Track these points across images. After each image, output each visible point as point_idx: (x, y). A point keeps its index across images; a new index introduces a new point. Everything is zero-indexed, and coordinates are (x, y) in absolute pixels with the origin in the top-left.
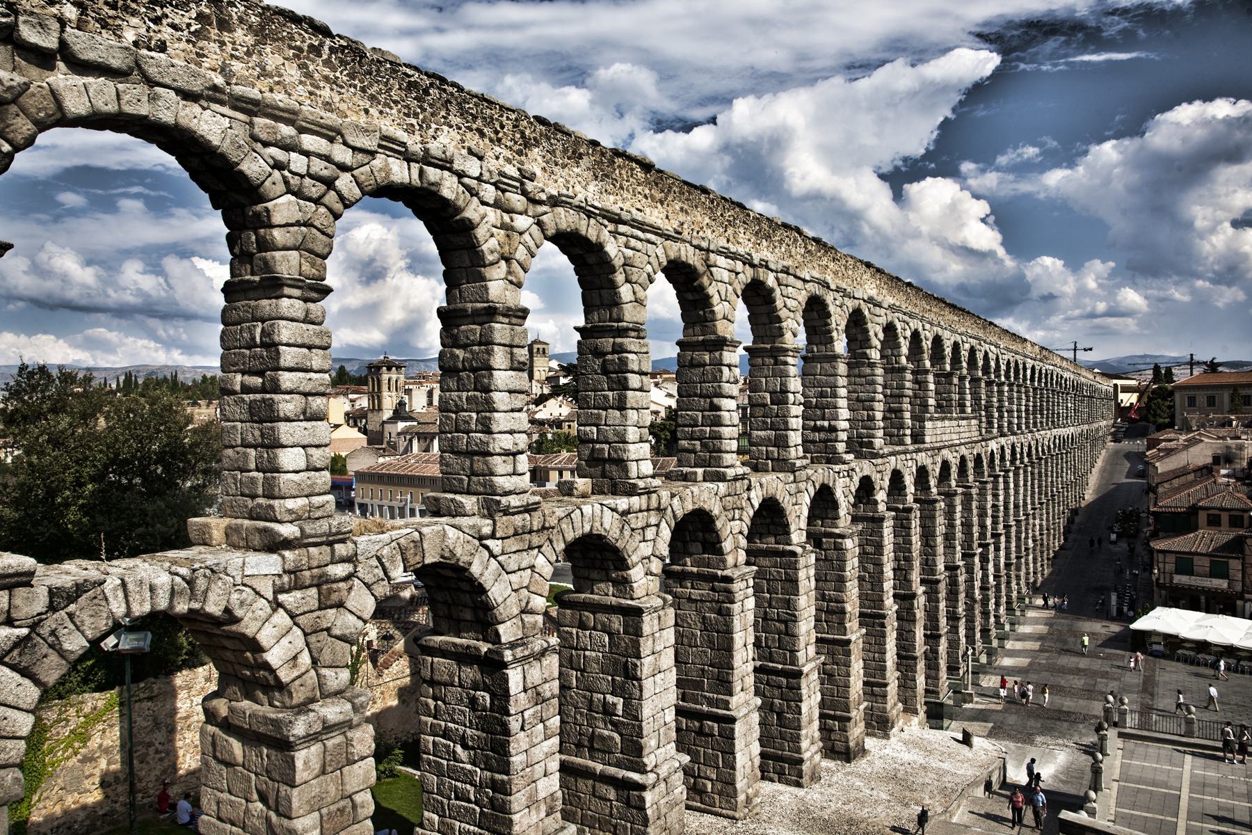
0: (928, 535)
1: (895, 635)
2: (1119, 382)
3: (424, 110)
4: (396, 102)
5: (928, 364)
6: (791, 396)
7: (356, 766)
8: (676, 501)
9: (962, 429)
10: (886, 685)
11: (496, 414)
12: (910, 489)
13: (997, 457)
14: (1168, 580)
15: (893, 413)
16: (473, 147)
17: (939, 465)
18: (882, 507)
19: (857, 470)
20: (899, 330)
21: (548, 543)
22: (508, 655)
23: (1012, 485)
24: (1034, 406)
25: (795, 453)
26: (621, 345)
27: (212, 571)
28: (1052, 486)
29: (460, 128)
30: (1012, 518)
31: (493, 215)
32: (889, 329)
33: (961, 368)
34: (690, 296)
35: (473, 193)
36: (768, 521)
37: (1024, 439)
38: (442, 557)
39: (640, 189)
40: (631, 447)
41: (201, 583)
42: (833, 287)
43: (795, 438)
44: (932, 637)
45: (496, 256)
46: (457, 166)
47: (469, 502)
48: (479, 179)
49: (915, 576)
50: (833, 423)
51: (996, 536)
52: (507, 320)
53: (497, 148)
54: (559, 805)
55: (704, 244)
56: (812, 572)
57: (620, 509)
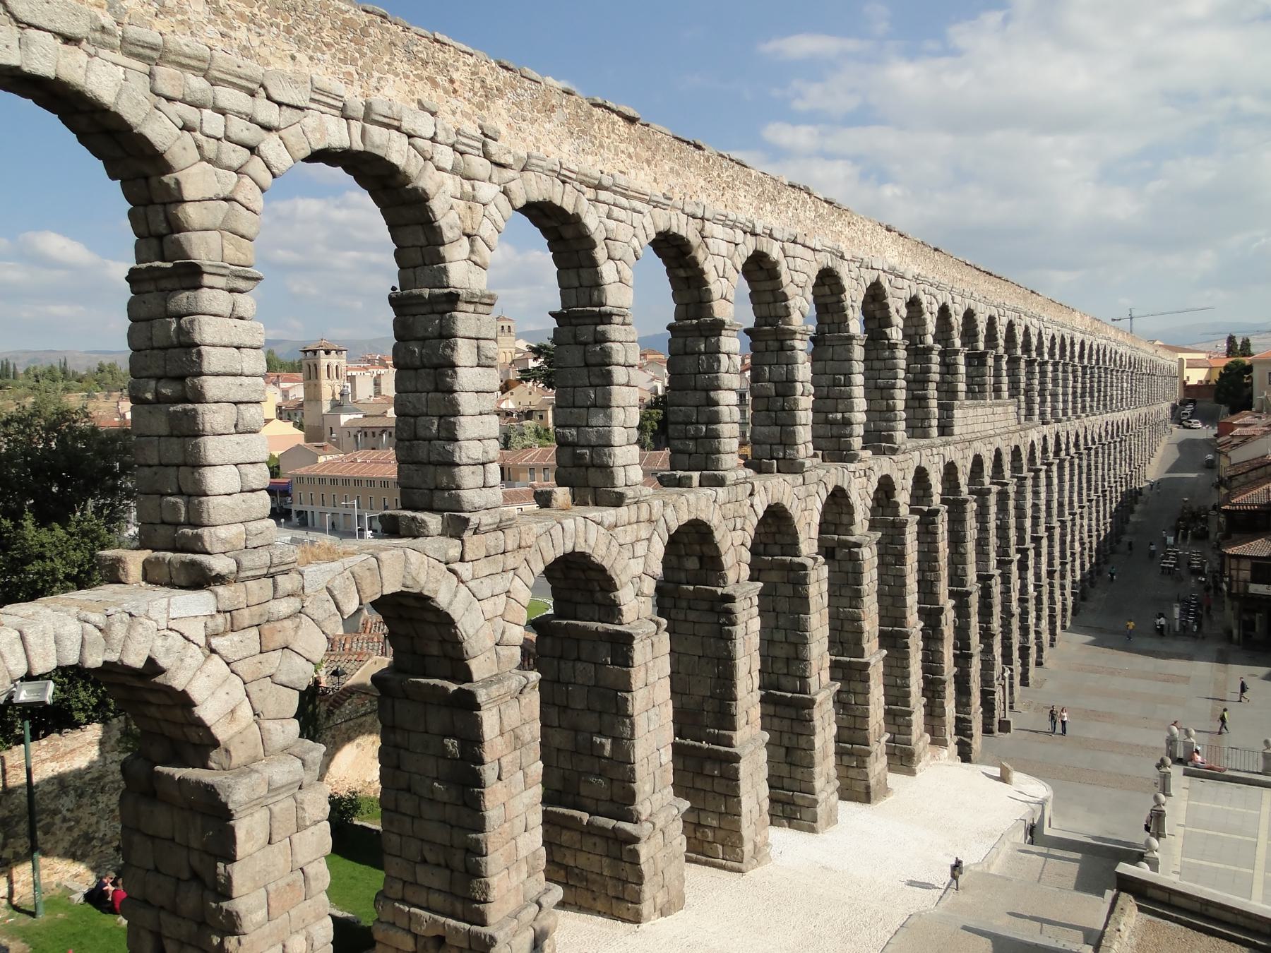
0: (956, 539)
1: (920, 657)
2: (1185, 356)
3: (363, 55)
4: (327, 45)
5: (958, 343)
6: (799, 386)
7: (308, 832)
9: (997, 418)
10: (910, 714)
12: (937, 488)
14: (1241, 590)
15: (917, 402)
16: (425, 101)
17: (971, 460)
18: (904, 511)
19: (876, 468)
20: (924, 305)
22: (482, 696)
23: (1055, 481)
24: (1084, 388)
26: (603, 333)
27: (131, 615)
28: (1103, 480)
29: (408, 77)
30: (1055, 518)
31: (452, 184)
32: (914, 304)
33: (997, 346)
34: (682, 273)
36: (773, 529)
37: (1070, 427)
38: (404, 585)
39: (623, 146)
41: (119, 631)
42: (847, 256)
43: (804, 434)
44: (963, 658)
45: (457, 232)
46: (406, 126)
47: (433, 521)
48: (433, 140)
49: (943, 588)
50: (847, 415)
51: (1036, 540)
52: (471, 308)
53: (454, 101)
54: (542, 863)
55: (699, 213)
56: (825, 586)
57: (606, 523)
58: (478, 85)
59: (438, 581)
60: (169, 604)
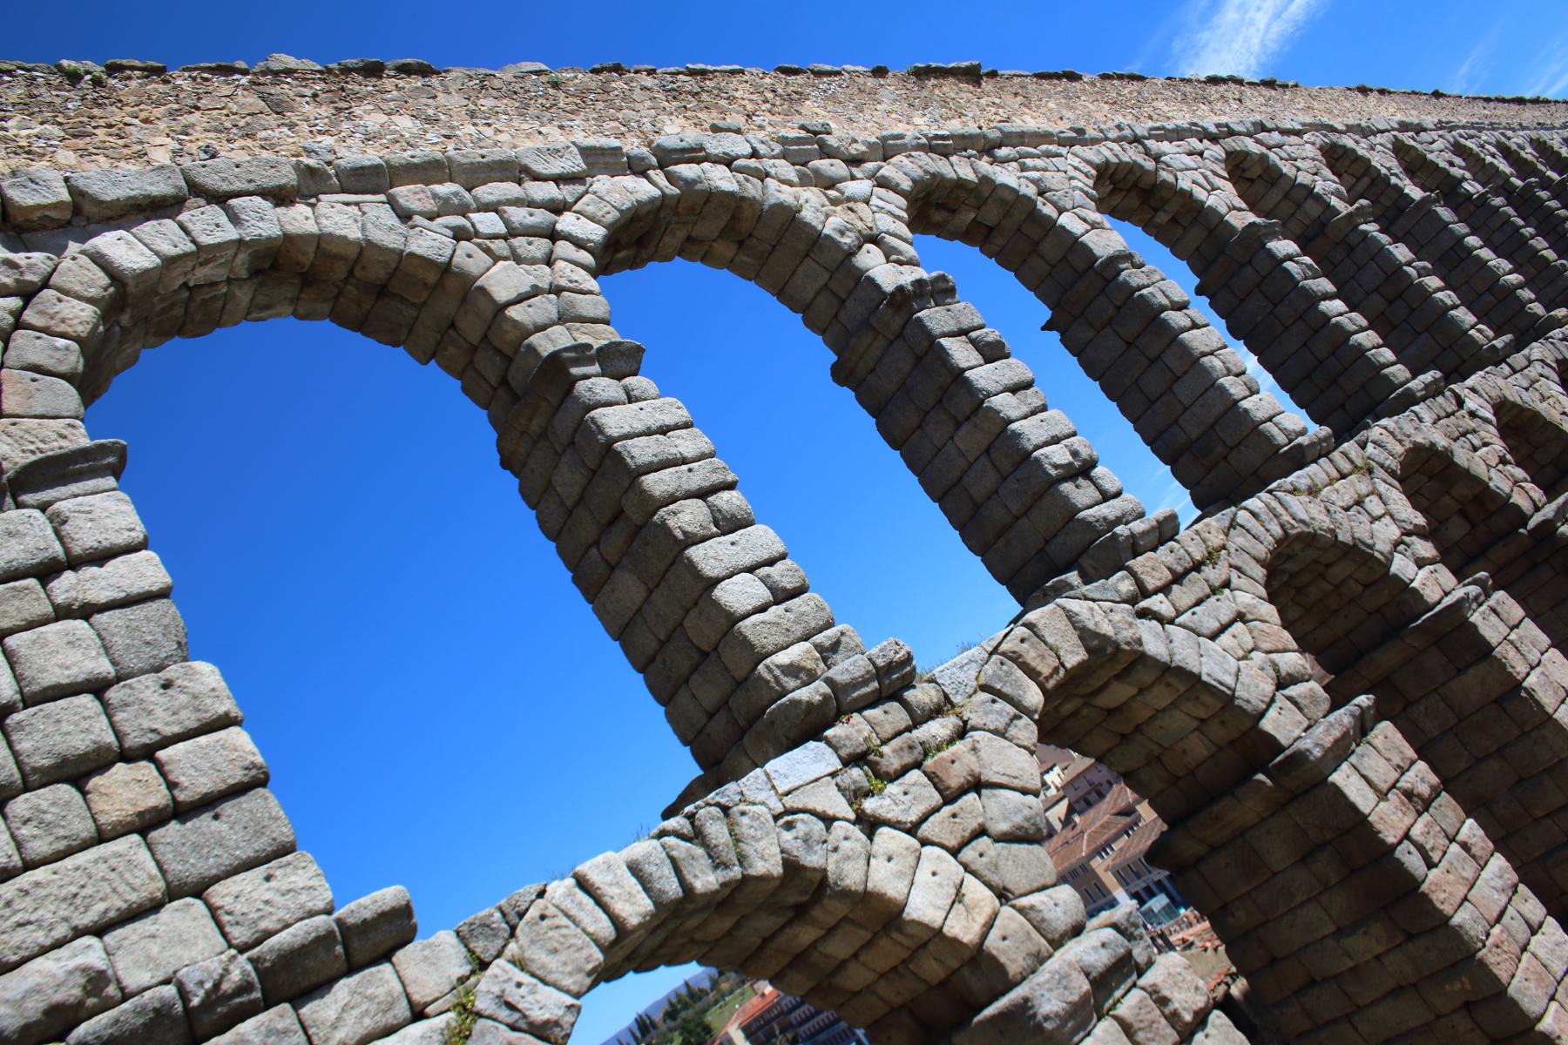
8: (1370, 447)
11: (1013, 426)
20: (1476, 149)
21: (1234, 574)
25: (1481, 334)
34: (1162, 218)
35: (763, 175)
39: (983, 101)
42: (1341, 127)
48: (755, 154)
55: (1127, 132)
58: (770, 95)
59: (1130, 625)
60: (768, 775)
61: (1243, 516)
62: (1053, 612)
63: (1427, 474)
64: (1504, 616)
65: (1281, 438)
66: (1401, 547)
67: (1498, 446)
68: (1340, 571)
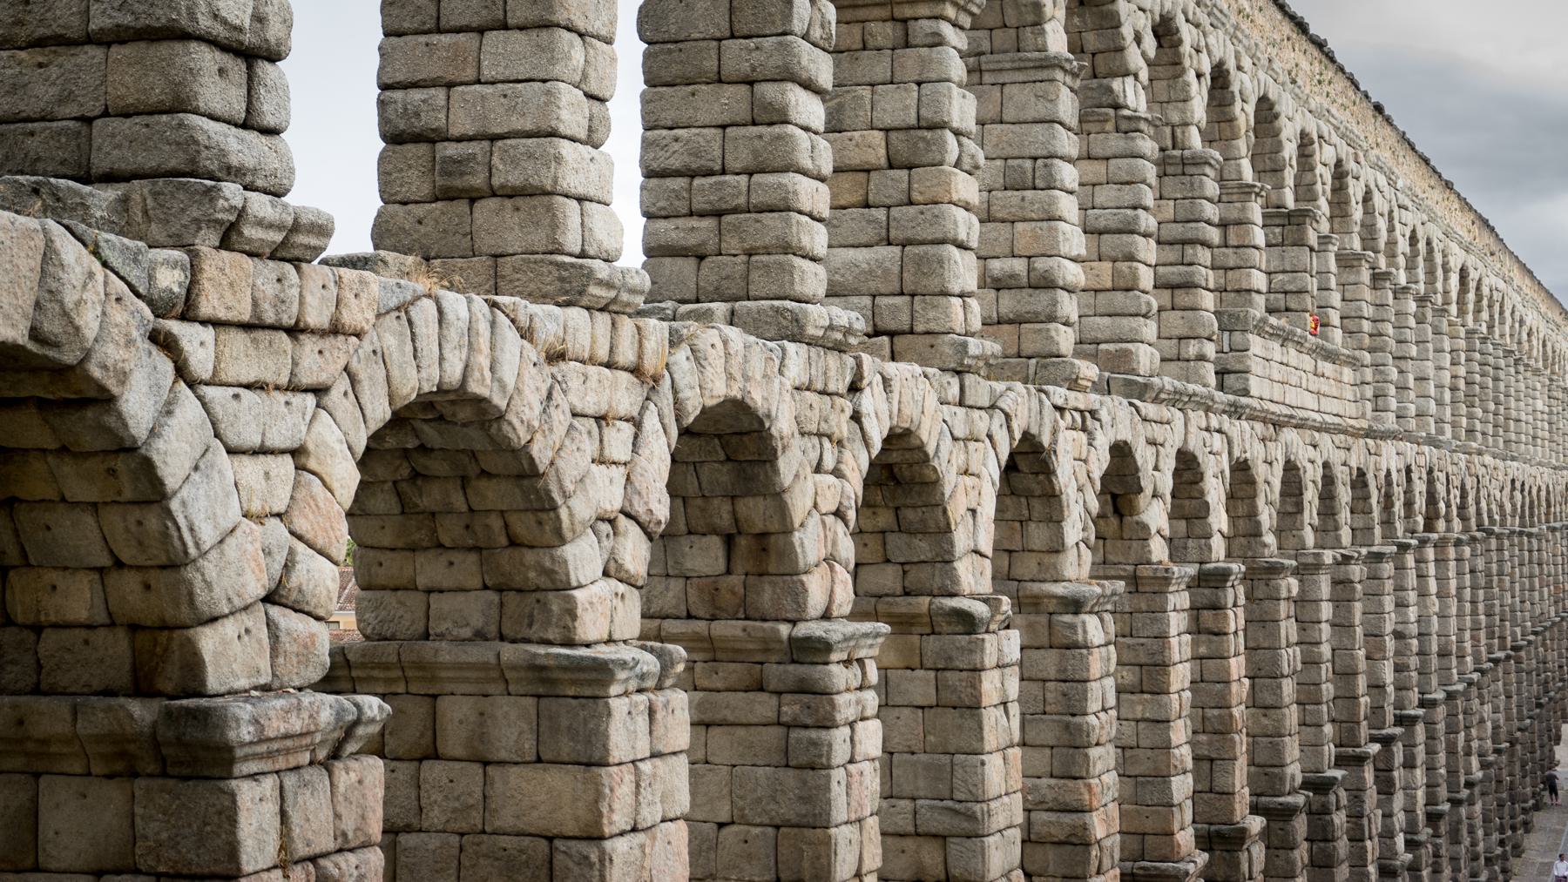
8: (683, 353)
12: (1219, 520)
13: (1398, 492)
18: (1158, 550)
20: (1186, 48)
21: (343, 384)
25: (964, 315)
32: (1165, 31)
40: (566, 147)
43: (963, 271)
50: (1040, 264)
56: (1014, 687)
59: (130, 342)
61: (425, 312)
62: (28, 234)
63: (726, 451)
64: (659, 730)
65: (572, 241)
66: (605, 528)
67: (854, 486)
68: (493, 494)
